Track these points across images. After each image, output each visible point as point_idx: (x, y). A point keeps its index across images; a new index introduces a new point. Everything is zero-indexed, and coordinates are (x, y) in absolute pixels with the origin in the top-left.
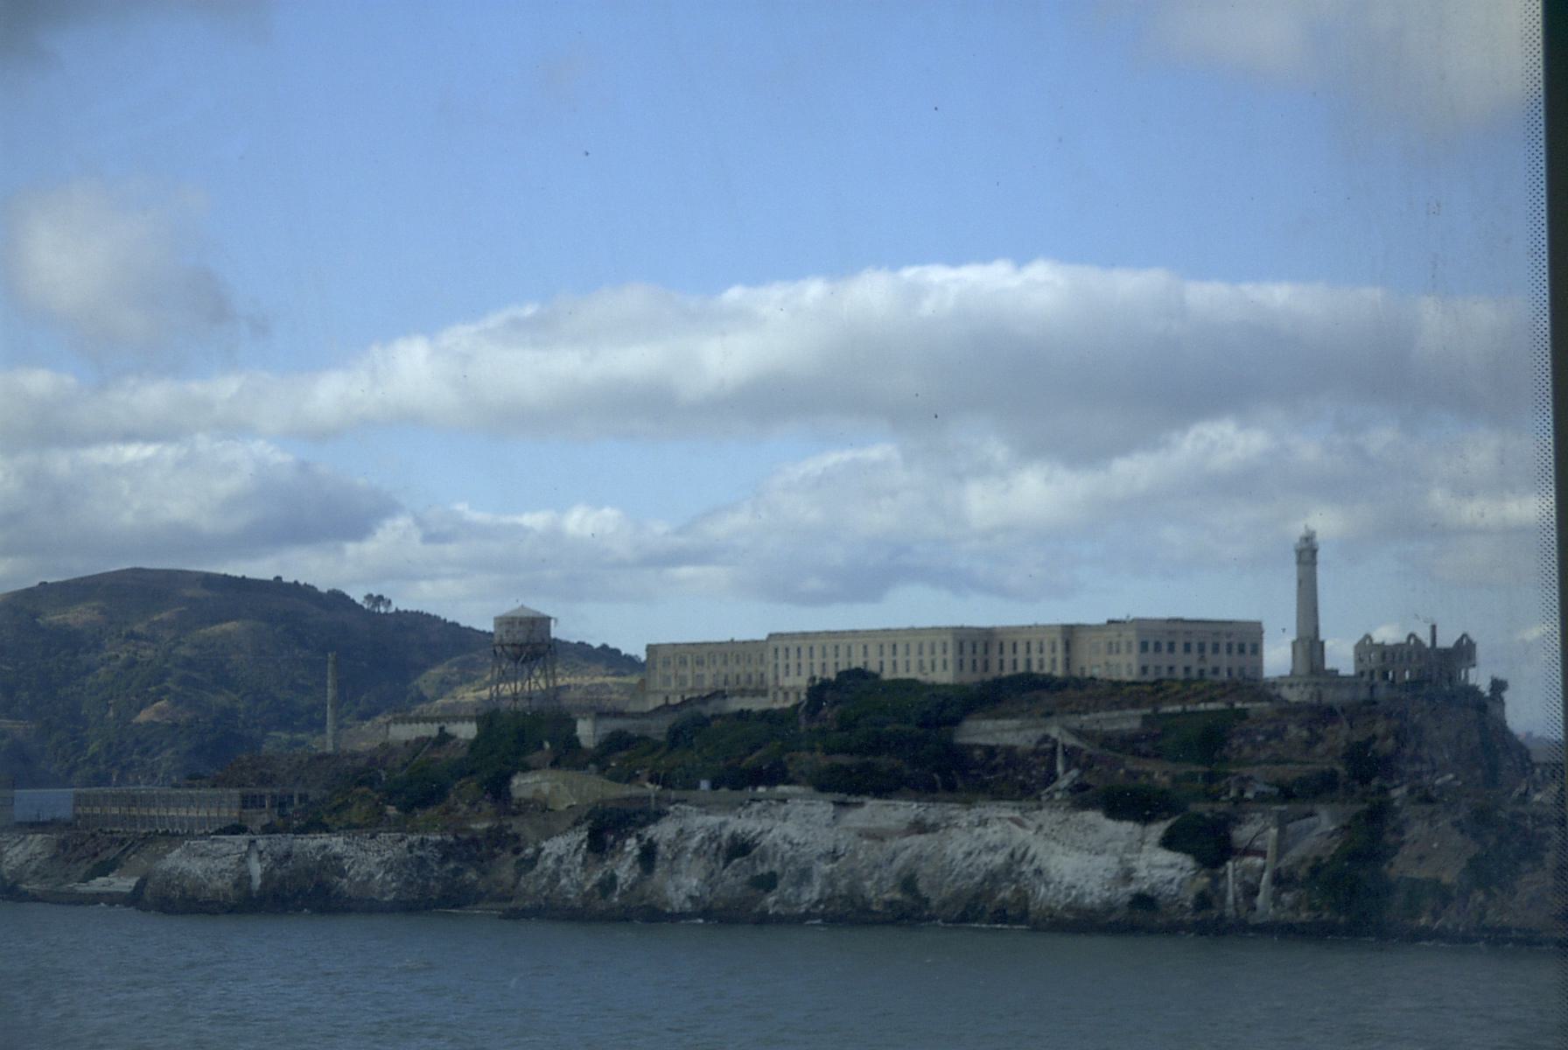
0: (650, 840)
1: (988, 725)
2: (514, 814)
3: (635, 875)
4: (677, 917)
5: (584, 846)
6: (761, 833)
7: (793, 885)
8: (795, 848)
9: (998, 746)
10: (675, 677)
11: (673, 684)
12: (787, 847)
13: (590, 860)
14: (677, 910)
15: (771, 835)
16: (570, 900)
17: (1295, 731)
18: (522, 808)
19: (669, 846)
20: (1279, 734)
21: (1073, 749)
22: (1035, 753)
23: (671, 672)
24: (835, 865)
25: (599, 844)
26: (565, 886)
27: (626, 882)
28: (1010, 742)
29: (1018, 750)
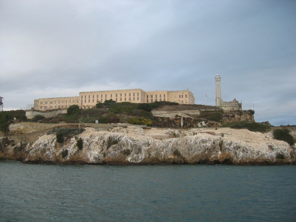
0: (80, 138)
1: (158, 112)
2: (11, 135)
3: (75, 150)
4: (289, 163)
5: (55, 140)
6: (120, 137)
7: (136, 153)
8: (134, 141)
9: (164, 117)
10: (44, 106)
11: (43, 107)
12: (131, 141)
13: (58, 146)
14: (91, 162)
15: (124, 137)
16: (50, 158)
17: (237, 116)
18: (14, 133)
19: (87, 141)
20: (233, 116)
21: (188, 118)
22: (176, 119)
23: (43, 105)
24: (149, 147)
25: (61, 138)
26: (48, 154)
27: (73, 152)
28: (168, 117)
29: (170, 118)
